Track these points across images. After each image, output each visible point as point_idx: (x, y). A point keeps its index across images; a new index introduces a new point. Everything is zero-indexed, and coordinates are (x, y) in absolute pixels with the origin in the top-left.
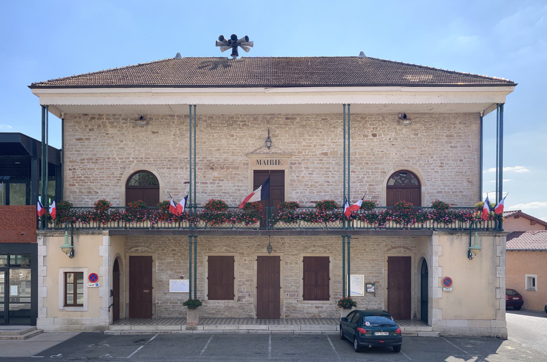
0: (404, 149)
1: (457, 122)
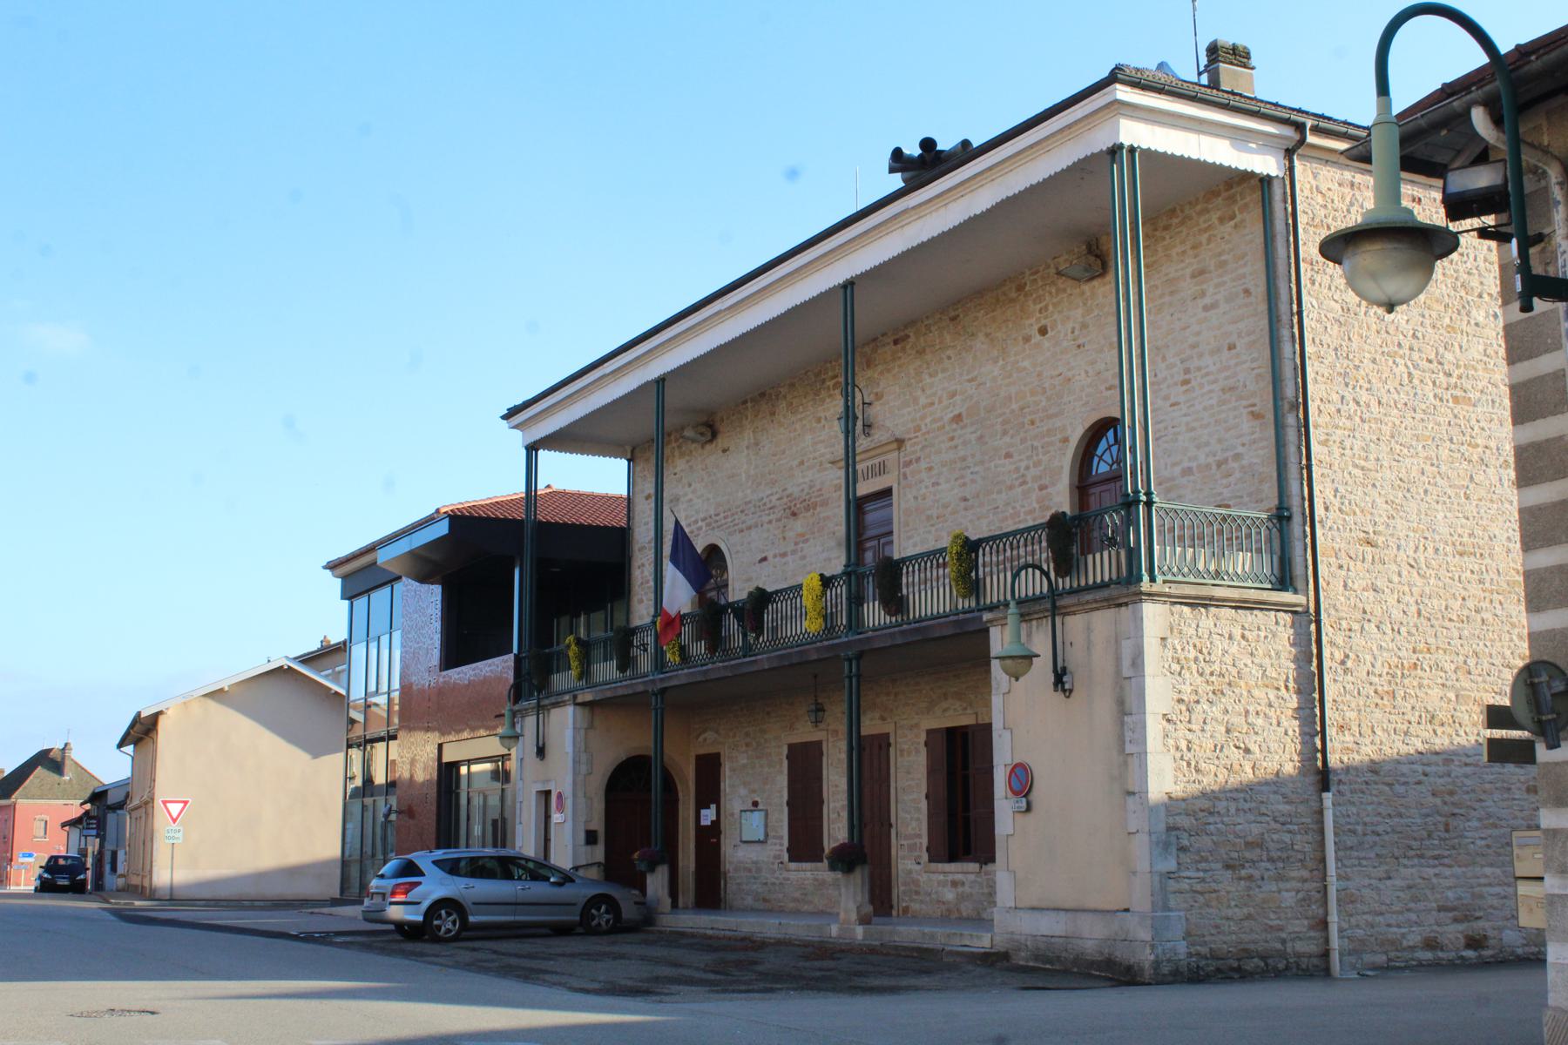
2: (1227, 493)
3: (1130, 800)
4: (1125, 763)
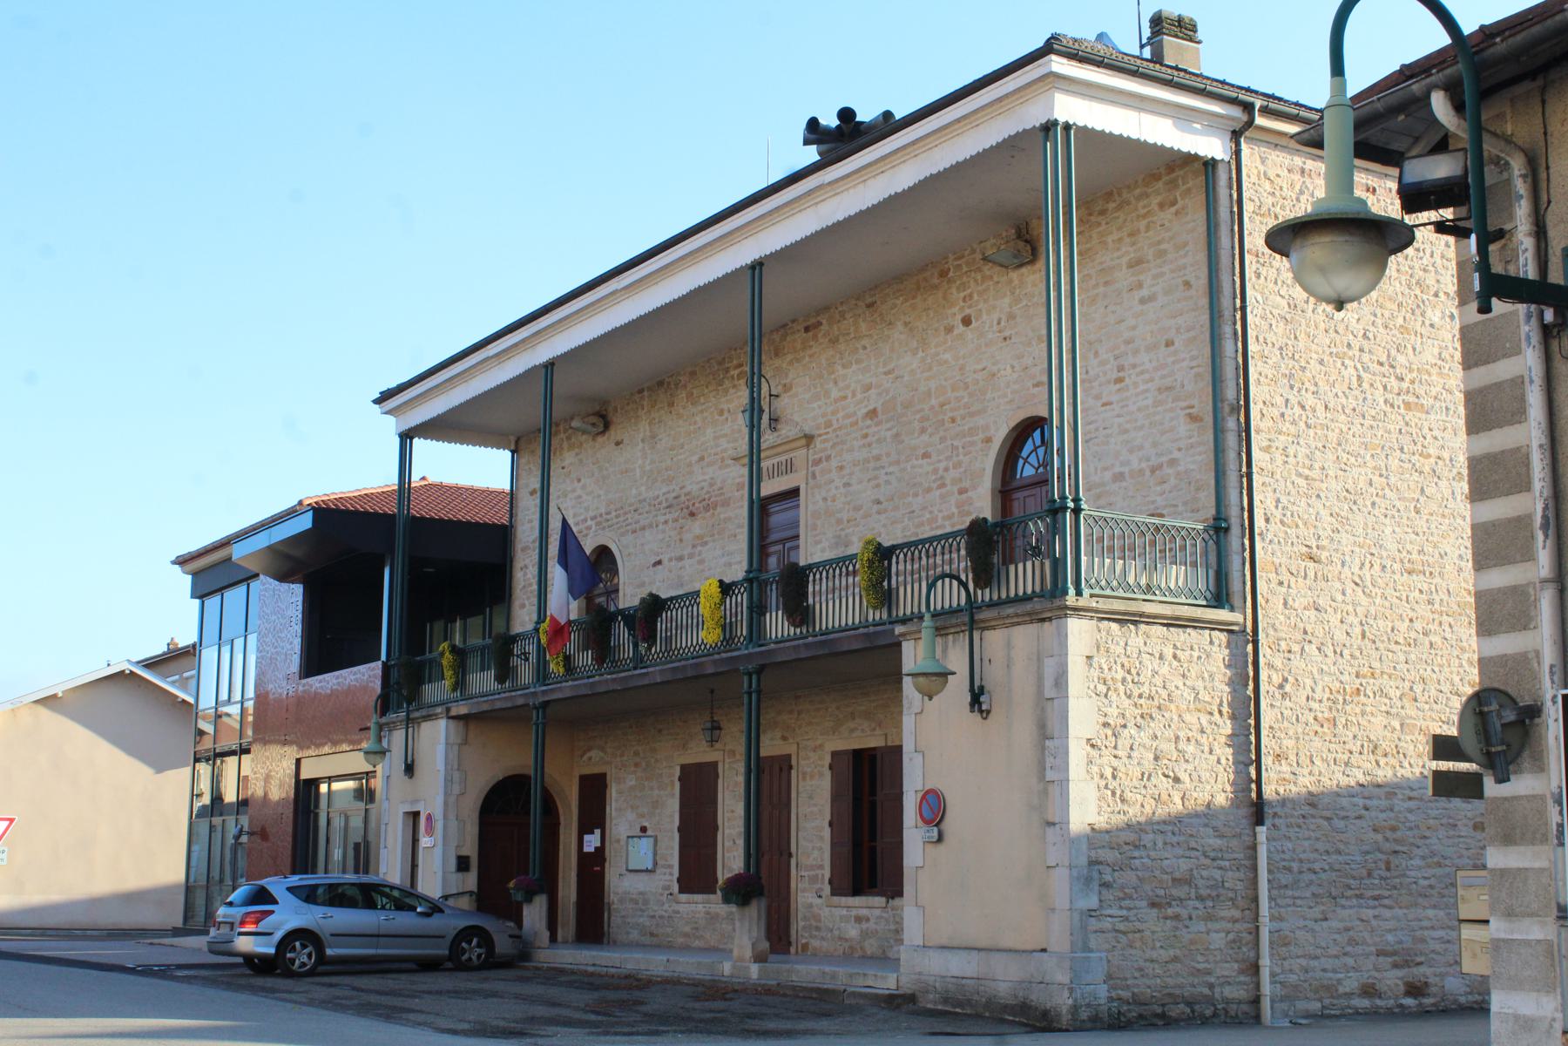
0: (1029, 344)
1: (1154, 205)
2: (1160, 501)
3: (1050, 831)
4: (1045, 792)
